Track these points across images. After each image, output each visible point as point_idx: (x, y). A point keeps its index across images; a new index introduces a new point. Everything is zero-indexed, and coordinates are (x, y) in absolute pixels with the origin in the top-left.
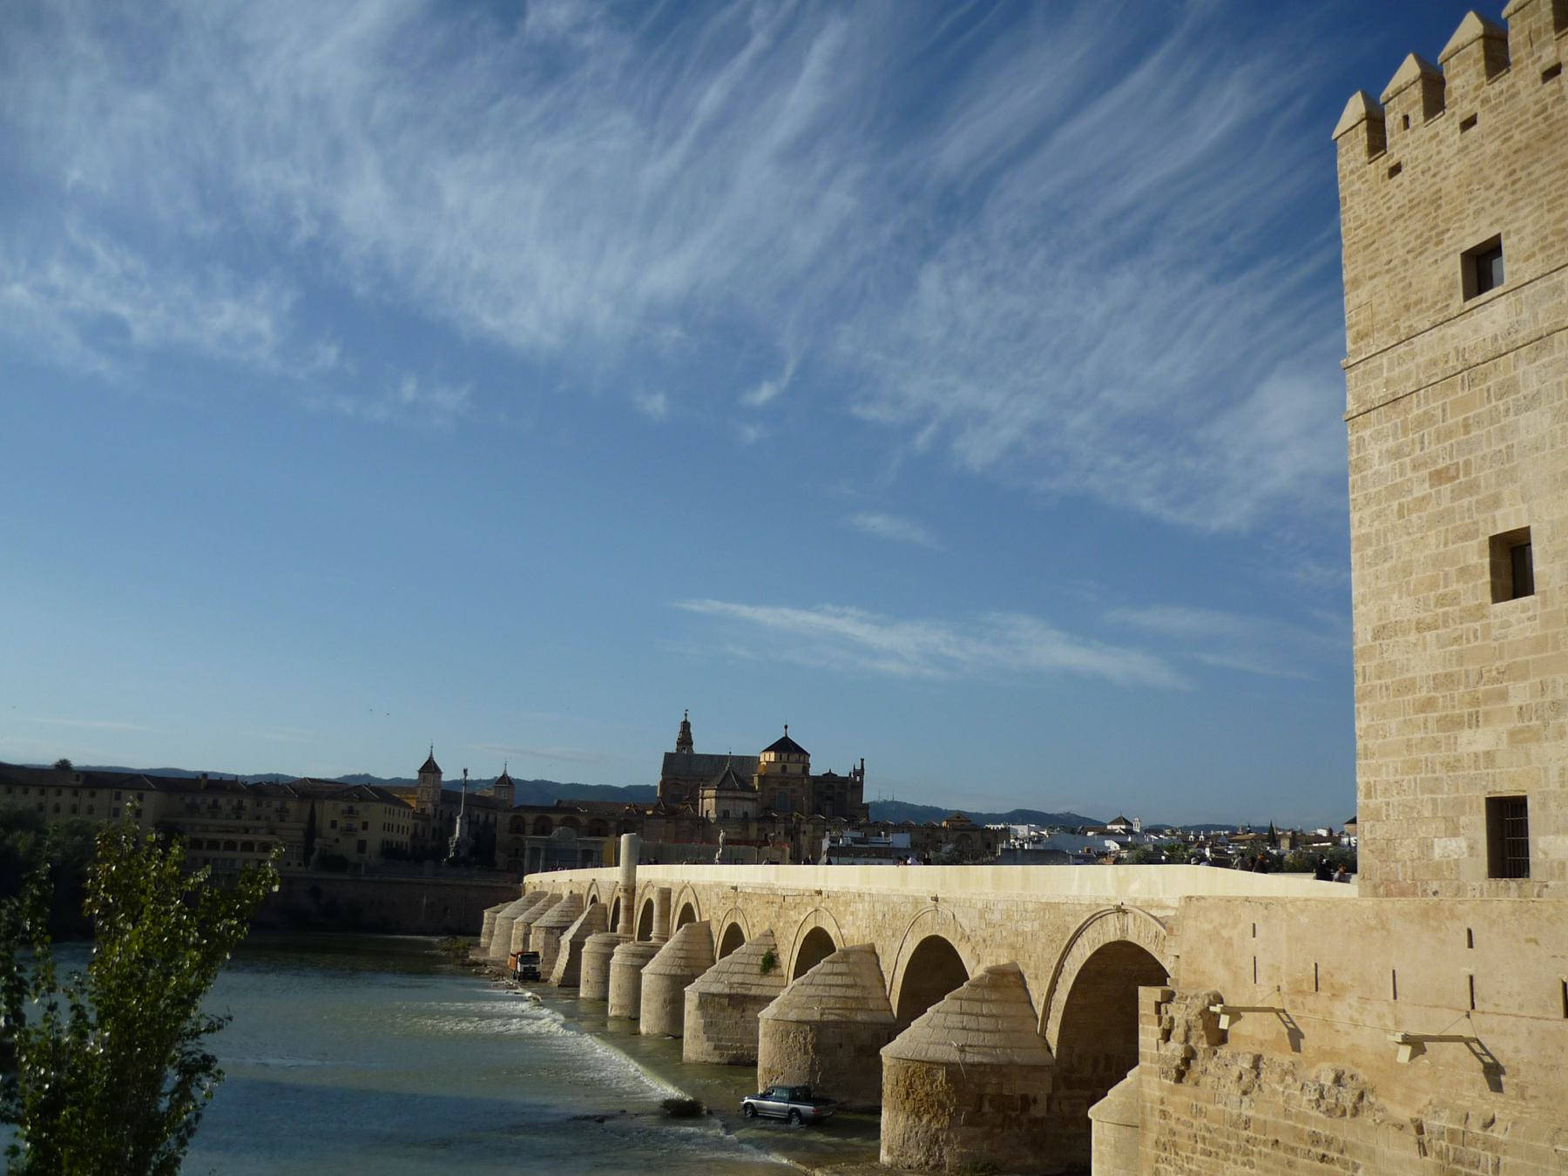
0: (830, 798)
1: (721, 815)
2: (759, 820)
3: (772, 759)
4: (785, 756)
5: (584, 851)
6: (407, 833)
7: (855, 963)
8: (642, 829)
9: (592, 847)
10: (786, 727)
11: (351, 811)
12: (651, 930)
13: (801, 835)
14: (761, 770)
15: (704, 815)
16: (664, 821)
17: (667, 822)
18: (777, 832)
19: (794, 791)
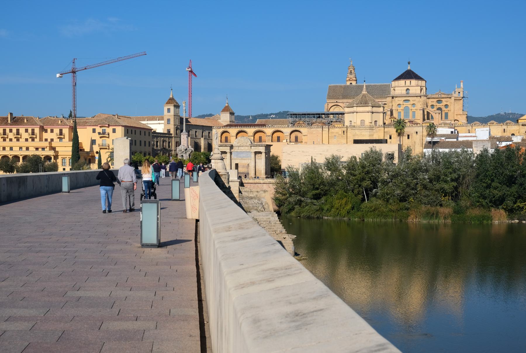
0: (440, 109)
4: (408, 82)
6: (149, 146)
10: (409, 63)
11: (104, 133)
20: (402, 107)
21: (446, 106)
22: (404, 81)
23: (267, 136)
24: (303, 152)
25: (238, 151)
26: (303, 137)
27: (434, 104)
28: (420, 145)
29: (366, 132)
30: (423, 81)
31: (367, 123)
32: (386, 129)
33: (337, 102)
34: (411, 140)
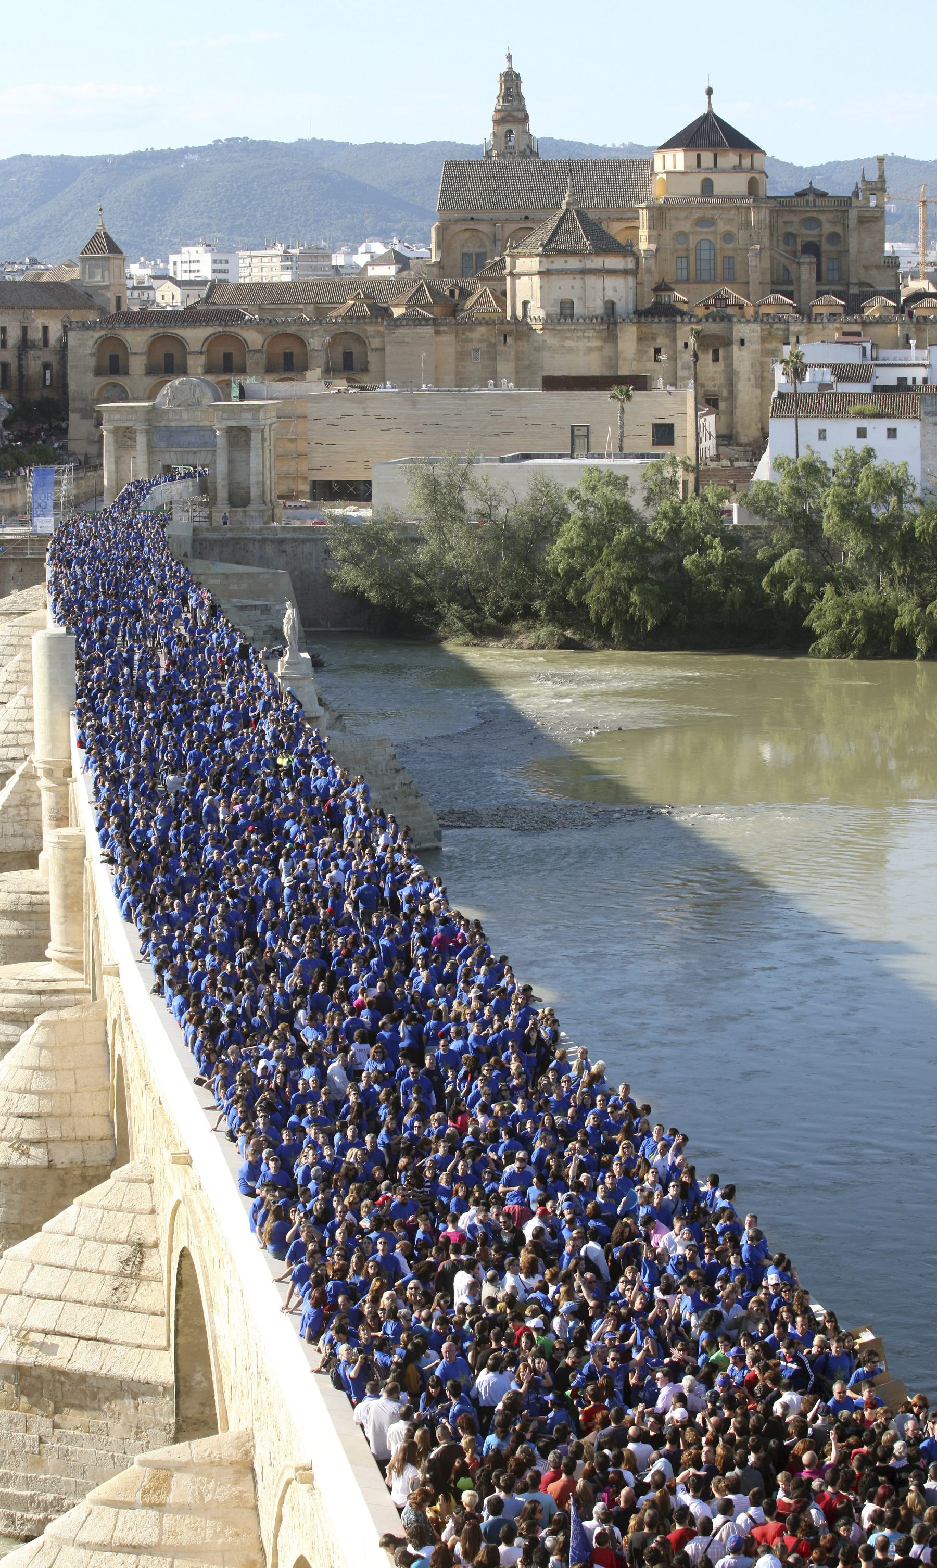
0: (812, 248)
1: (556, 310)
2: (642, 314)
3: (680, 167)
4: (707, 158)
5: (230, 430)
7: (182, 1509)
8: (383, 350)
9: (246, 420)
10: (710, 92)
12: (48, 939)
13: (735, 348)
14: (657, 192)
15: (519, 313)
16: (429, 330)
17: (437, 332)
18: (680, 344)
19: (728, 237)
20: (693, 241)
21: (834, 238)
22: (694, 155)
23: (250, 351)
24: (378, 417)
25: (173, 424)
26: (372, 358)
27: (793, 229)
28: (753, 381)
29: (578, 338)
30: (756, 155)
31: (578, 309)
32: (644, 329)
33: (472, 219)
34: (726, 365)
